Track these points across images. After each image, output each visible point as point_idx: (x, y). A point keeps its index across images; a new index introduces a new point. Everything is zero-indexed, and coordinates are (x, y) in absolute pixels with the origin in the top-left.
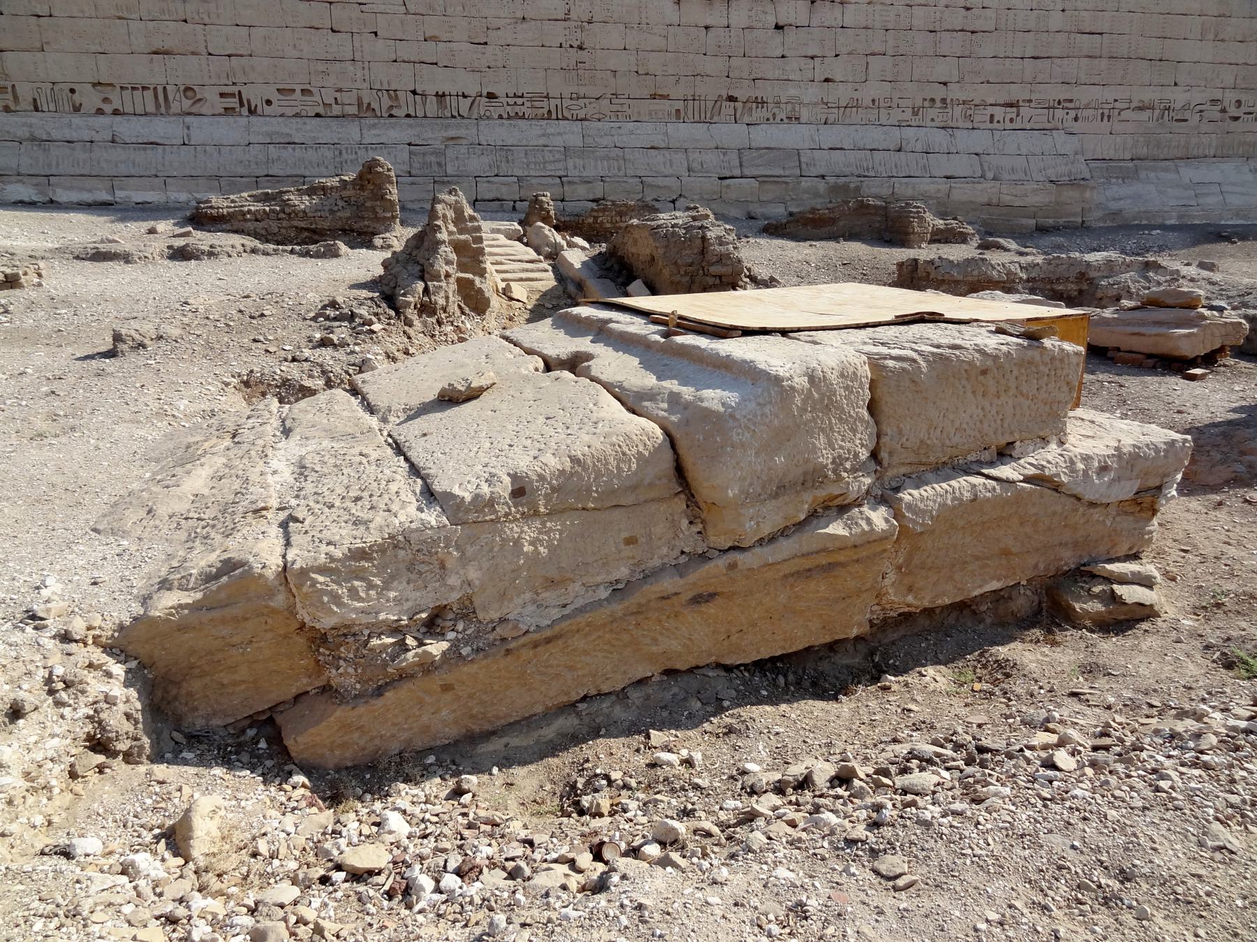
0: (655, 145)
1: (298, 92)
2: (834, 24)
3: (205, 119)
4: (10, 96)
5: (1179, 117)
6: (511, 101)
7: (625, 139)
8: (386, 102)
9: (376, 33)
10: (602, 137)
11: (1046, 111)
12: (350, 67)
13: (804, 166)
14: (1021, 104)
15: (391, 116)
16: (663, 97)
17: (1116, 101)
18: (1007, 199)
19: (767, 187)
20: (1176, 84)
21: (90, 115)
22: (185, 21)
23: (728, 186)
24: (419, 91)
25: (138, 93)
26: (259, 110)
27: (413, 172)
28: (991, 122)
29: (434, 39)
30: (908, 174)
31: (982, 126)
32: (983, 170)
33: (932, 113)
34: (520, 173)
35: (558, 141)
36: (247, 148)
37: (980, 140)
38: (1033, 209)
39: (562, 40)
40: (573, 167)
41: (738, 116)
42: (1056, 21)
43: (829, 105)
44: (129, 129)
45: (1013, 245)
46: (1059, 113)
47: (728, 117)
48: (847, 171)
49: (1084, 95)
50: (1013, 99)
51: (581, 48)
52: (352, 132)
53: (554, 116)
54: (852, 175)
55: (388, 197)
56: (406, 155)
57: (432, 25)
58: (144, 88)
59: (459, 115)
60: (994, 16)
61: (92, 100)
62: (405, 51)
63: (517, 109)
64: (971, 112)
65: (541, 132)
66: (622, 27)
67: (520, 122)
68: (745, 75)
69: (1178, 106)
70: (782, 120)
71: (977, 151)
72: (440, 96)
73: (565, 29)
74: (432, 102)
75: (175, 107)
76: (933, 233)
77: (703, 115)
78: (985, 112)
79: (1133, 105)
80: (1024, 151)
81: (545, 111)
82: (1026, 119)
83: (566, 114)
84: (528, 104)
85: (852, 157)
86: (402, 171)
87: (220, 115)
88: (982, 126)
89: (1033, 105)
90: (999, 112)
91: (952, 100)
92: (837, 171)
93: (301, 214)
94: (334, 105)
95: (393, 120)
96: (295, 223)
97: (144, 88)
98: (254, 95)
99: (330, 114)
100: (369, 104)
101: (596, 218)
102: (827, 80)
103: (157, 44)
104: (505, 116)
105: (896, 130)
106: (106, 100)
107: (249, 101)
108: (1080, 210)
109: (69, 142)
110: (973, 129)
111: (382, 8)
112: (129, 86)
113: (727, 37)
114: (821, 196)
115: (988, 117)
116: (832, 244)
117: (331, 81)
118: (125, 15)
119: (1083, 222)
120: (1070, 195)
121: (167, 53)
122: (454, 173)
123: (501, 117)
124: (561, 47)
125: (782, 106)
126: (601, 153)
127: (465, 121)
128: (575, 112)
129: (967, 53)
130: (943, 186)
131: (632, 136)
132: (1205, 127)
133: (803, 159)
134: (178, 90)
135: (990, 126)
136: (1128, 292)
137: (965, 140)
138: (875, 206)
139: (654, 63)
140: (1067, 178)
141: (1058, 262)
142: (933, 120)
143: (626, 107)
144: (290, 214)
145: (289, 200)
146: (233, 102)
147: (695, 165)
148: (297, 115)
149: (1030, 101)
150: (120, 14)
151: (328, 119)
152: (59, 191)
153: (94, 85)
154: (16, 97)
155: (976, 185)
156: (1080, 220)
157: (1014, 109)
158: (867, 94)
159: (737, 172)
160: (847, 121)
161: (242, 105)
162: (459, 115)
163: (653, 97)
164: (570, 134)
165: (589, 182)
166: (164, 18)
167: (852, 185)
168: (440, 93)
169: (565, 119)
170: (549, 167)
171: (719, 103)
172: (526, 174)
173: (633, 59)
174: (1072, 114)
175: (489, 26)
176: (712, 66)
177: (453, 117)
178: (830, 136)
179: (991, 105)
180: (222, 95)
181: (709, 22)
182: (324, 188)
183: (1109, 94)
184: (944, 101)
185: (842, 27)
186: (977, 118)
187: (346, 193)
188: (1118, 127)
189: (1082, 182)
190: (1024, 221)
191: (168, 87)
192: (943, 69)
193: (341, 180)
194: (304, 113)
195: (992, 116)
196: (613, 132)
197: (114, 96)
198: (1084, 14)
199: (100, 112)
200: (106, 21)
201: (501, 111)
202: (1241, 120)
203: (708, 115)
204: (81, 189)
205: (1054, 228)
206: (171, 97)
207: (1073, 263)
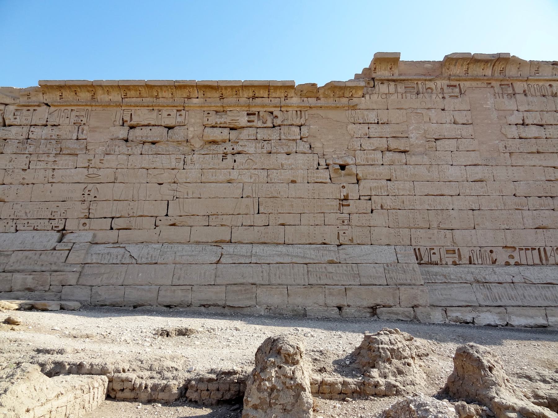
4: (456, 255)
21: (502, 266)
22: (553, 210)
44: (533, 274)
58: (533, 249)
61: (502, 256)
97: (533, 249)
103: (539, 223)
106: (512, 257)
109: (499, 283)
112: (524, 248)
118: (520, 208)
150: (518, 207)
152: (513, 317)
153: (503, 247)
154: (460, 256)
166: (542, 208)
191: (546, 248)
197: (516, 254)
199: (507, 264)
200: (510, 211)
204: (526, 316)
206: (549, 254)
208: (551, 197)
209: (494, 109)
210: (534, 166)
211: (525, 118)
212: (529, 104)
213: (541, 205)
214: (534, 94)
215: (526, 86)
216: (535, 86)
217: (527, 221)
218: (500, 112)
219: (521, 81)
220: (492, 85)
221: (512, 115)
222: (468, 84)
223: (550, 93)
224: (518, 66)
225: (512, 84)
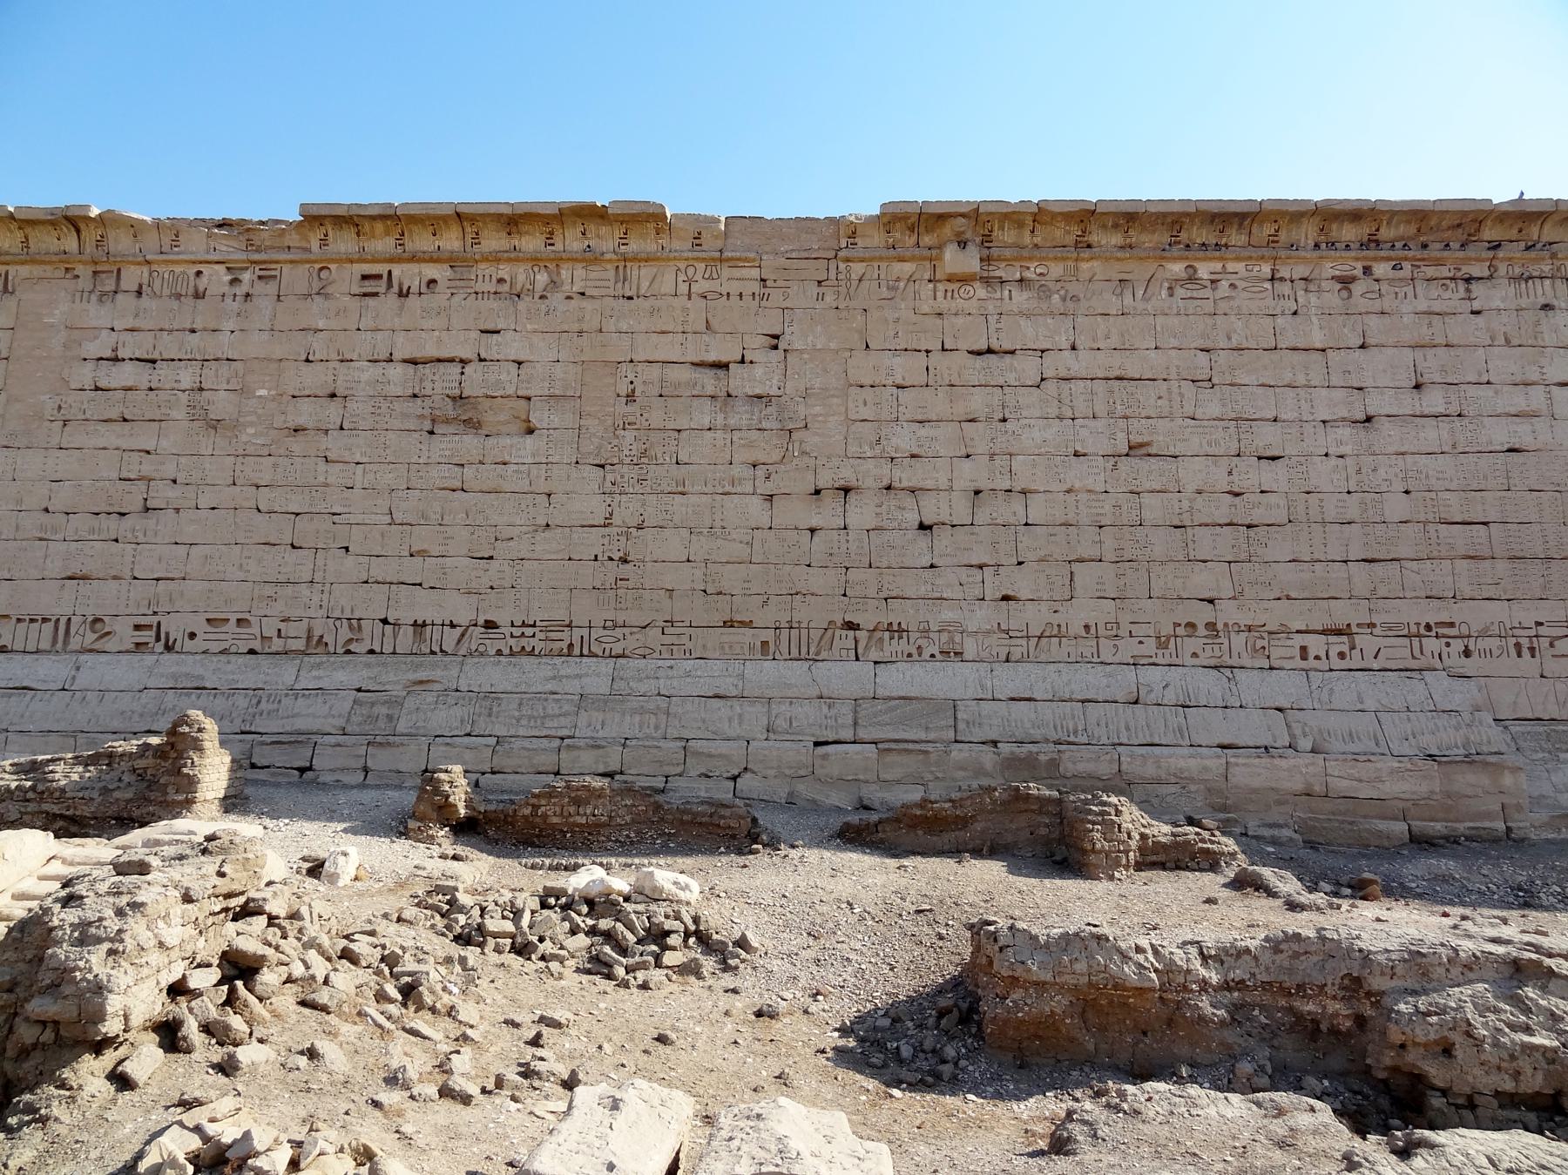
0: (722, 692)
1: (233, 621)
2: (1012, 520)
3: (103, 658)
6: (517, 632)
7: (675, 683)
8: (345, 633)
9: (347, 549)
10: (640, 680)
11: (1407, 641)
12: (304, 590)
13: (961, 726)
14: (1354, 629)
15: (348, 652)
16: (743, 624)
17: (1539, 624)
18: (1341, 785)
19: (889, 758)
22: (117, 541)
23: (825, 757)
24: (391, 620)
25: (36, 626)
26: (178, 647)
27: (349, 729)
28: (1304, 657)
29: (422, 553)
30: (1149, 740)
31: (1287, 664)
32: (1292, 736)
33: (1192, 644)
34: (502, 732)
35: (573, 686)
36: (138, 694)
37: (1286, 687)
38: (1401, 805)
39: (598, 550)
40: (587, 724)
41: (860, 651)
42: (1396, 507)
43: (1011, 634)
45: (1289, 884)
46: (1431, 644)
47: (844, 653)
48: (1037, 734)
49: (1474, 616)
50: (1341, 623)
51: (624, 561)
52: (286, 673)
53: (577, 651)
54: (1047, 741)
55: (185, 770)
56: (348, 705)
57: (422, 538)
58: (45, 620)
59: (442, 651)
60: (1282, 502)
62: (379, 570)
63: (524, 642)
64: (1265, 643)
65: (550, 674)
66: (685, 533)
67: (524, 660)
68: (872, 592)
70: (933, 656)
71: (1277, 704)
72: (419, 626)
73: (604, 536)
74: (406, 637)
75: (75, 643)
76: (1142, 850)
77: (804, 650)
78: (1289, 643)
80: (1370, 704)
81: (564, 645)
82: (1369, 654)
83: (596, 649)
84: (542, 636)
85: (1047, 712)
86: (334, 726)
87: (127, 651)
88: (1287, 664)
89: (1376, 631)
90: (1316, 644)
91: (1226, 625)
92: (1019, 735)
93: (57, 794)
94: (275, 639)
95: (348, 658)
96: (45, 807)
97: (45, 620)
98: (174, 627)
99: (267, 650)
100: (322, 637)
101: (535, 807)
102: (1006, 598)
103: (75, 569)
104: (506, 651)
105: (1130, 673)
107: (167, 634)
108: (1498, 807)
110: (1271, 668)
111: (359, 518)
113: (843, 541)
114: (987, 774)
115: (1297, 652)
116: (949, 863)
117: (278, 608)
119: (1509, 829)
120: (1468, 780)
121: (84, 578)
122: (405, 731)
123: (499, 653)
124: (596, 559)
125: (931, 635)
126: (634, 703)
127: (447, 659)
128: (608, 647)
129: (1243, 556)
130: (1214, 762)
131: (688, 680)
133: (959, 716)
134: (84, 622)
135: (1304, 664)
136: (1469, 1034)
137: (1252, 685)
138: (1038, 798)
139: (730, 578)
140: (1462, 751)
141: (1295, 947)
142: (1195, 655)
143: (685, 639)
144: (43, 792)
145: (52, 772)
146: (147, 636)
147: (781, 723)
148: (224, 652)
149: (1372, 625)
151: (263, 657)
155: (1277, 761)
156: (1501, 826)
157: (1344, 639)
158: (1075, 616)
159: (847, 734)
160: (1043, 657)
161: (158, 639)
162: (442, 651)
163: (728, 624)
164: (595, 676)
165: (599, 747)
166: (91, 537)
167: (1042, 758)
168: (420, 622)
169: (592, 655)
170: (550, 724)
171: (830, 632)
172: (512, 732)
173: (699, 573)
174: (1458, 646)
175: (499, 536)
176: (817, 580)
177: (433, 653)
178: (1009, 680)
179: (1298, 632)
180: (137, 627)
181: (814, 523)
182: (111, 756)
183: (1525, 615)
184: (1211, 626)
185: (1026, 524)
186: (1276, 653)
187: (140, 763)
189: (1477, 758)
190: (1382, 825)
192: (1203, 580)
193: (147, 746)
194: (234, 649)
195: (1304, 649)
196: (661, 673)
198: (1447, 495)
201: (501, 645)
203: (812, 650)
205: (1446, 838)
206: (73, 631)
207: (1328, 949)
208: (123, 514)
209: (62, 327)
210: (105, 449)
211: (120, 345)
212: (137, 315)
213: (92, 531)
214: (158, 293)
215: (146, 275)
216: (166, 276)
217: (52, 562)
218: (76, 332)
219: (139, 264)
220: (76, 273)
221: (96, 338)
222: (24, 270)
223: (191, 290)
224: (132, 230)
225: (119, 270)
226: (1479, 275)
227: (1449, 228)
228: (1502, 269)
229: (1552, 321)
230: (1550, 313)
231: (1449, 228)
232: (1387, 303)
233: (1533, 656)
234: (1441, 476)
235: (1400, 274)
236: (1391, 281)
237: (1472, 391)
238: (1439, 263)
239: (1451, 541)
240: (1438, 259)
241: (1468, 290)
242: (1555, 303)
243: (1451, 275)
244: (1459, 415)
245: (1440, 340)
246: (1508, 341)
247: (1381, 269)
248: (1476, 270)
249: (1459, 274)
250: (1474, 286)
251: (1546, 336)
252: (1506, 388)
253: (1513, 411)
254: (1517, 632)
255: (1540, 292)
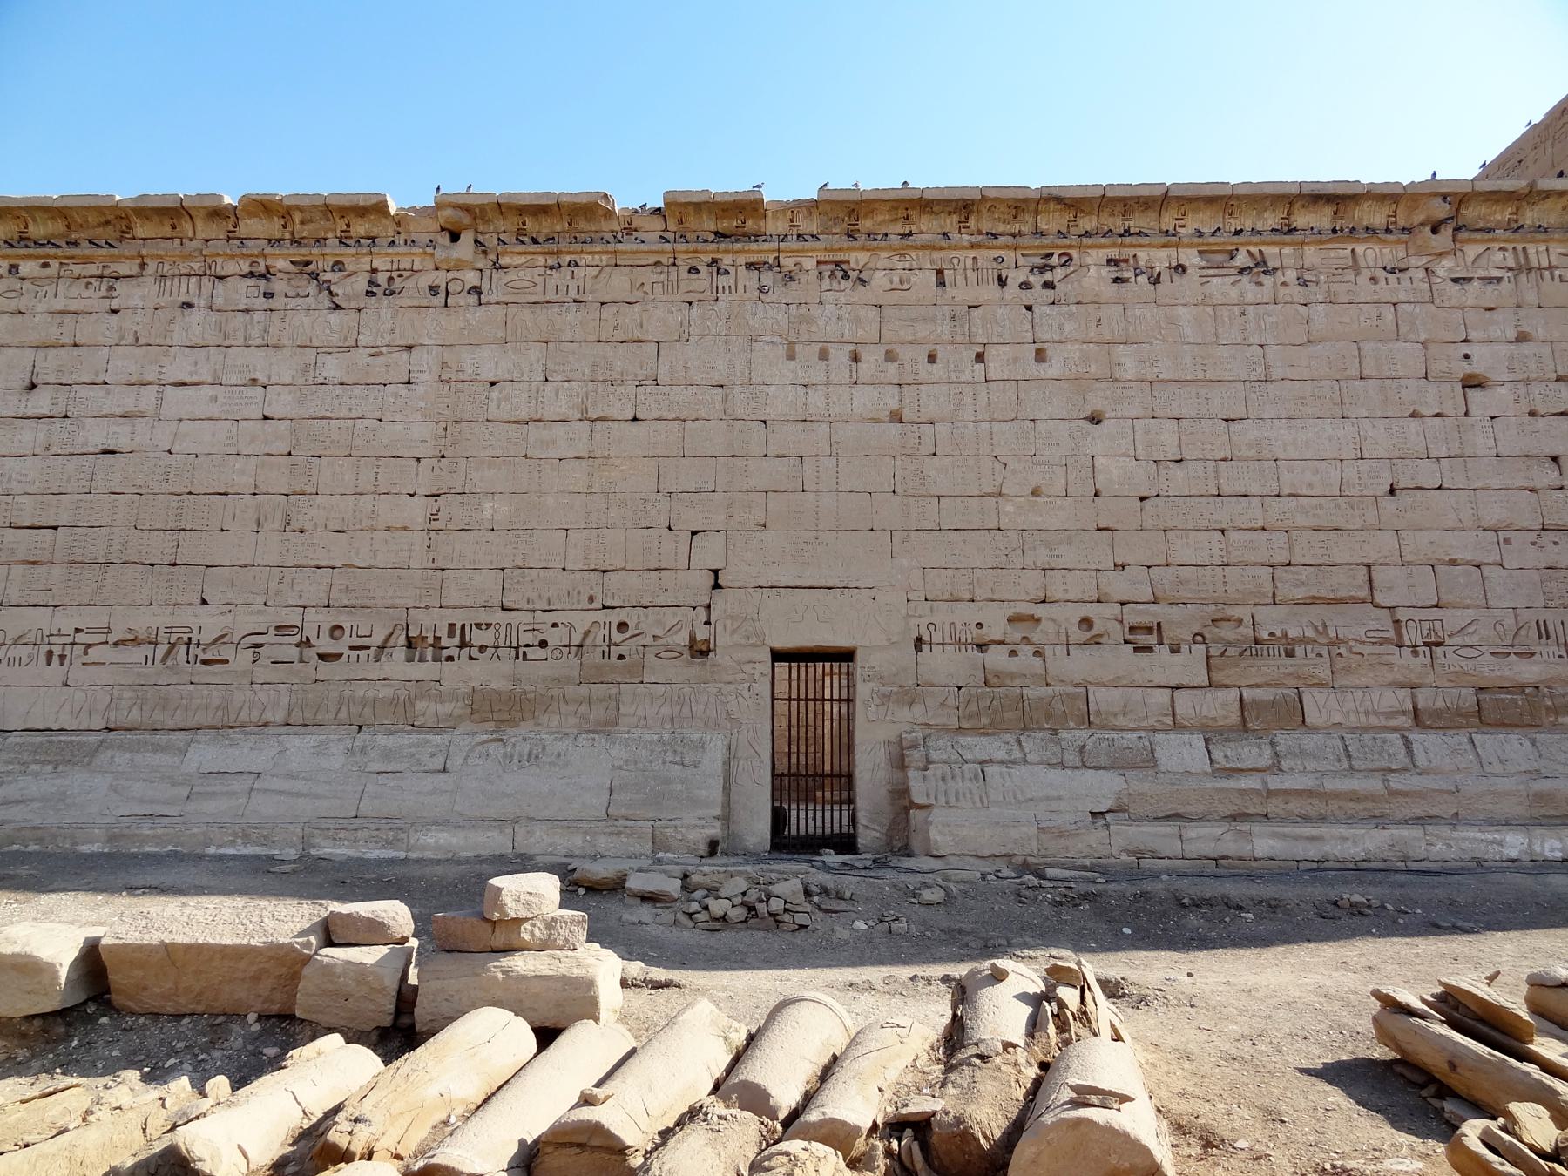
5: (208, 656)
17: (78, 630)
20: (204, 602)
69: (206, 638)
79: (112, 638)
132: (263, 672)
183: (65, 622)
188: (78, 674)
202: (344, 658)
226: (128, 273)
227: (99, 225)
228: (151, 267)
229: (187, 319)
230: (187, 311)
231: (99, 225)
232: (23, 303)
233: (62, 665)
234: (23, 479)
235: (47, 272)
236: (35, 280)
237: (83, 391)
238: (87, 260)
239: (15, 546)
240: (88, 257)
241: (111, 288)
242: (195, 301)
243: (97, 273)
244: (66, 417)
245: (66, 339)
246: (137, 340)
247: (27, 268)
248: (124, 268)
249: (106, 272)
250: (117, 285)
251: (176, 336)
252: (119, 388)
253: (118, 411)
254: (53, 640)
255: (184, 289)
